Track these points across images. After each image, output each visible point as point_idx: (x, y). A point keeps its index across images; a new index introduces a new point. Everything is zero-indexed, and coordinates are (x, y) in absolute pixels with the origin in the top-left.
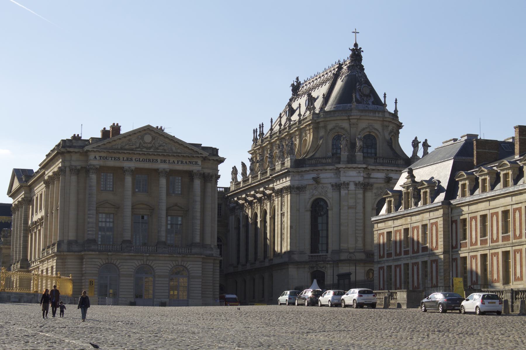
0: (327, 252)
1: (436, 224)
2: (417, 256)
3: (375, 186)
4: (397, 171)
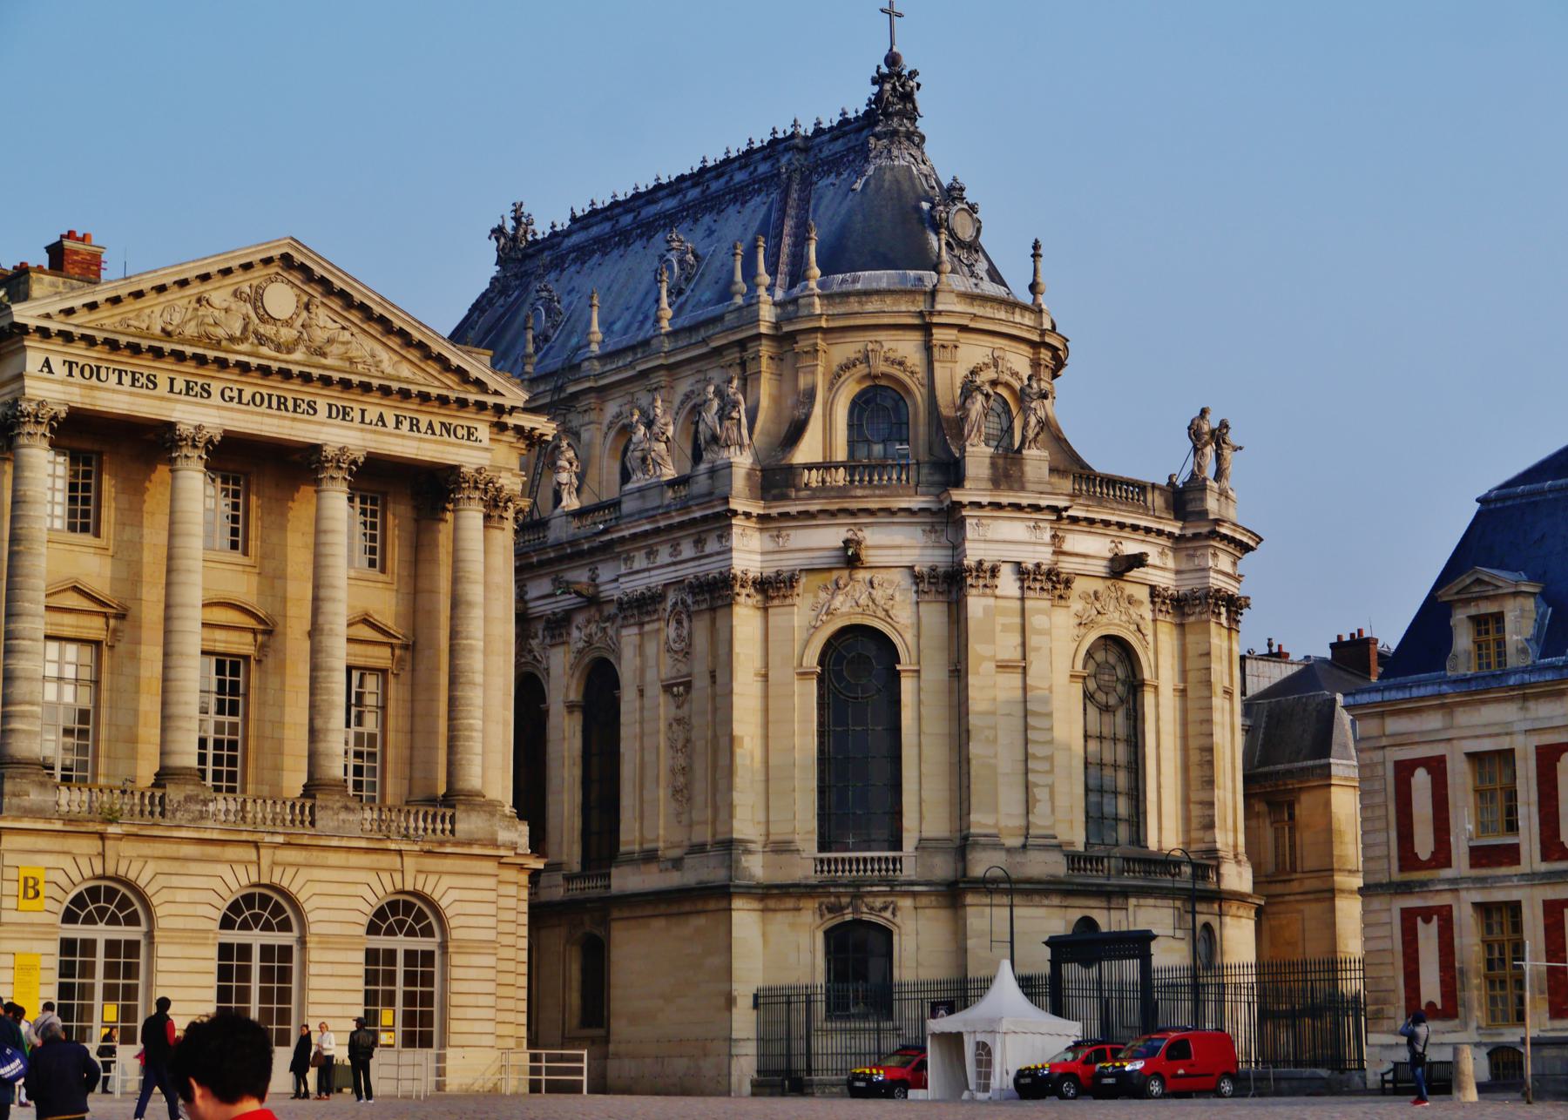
0: (897, 844)
3: (1079, 585)
4: (1148, 530)
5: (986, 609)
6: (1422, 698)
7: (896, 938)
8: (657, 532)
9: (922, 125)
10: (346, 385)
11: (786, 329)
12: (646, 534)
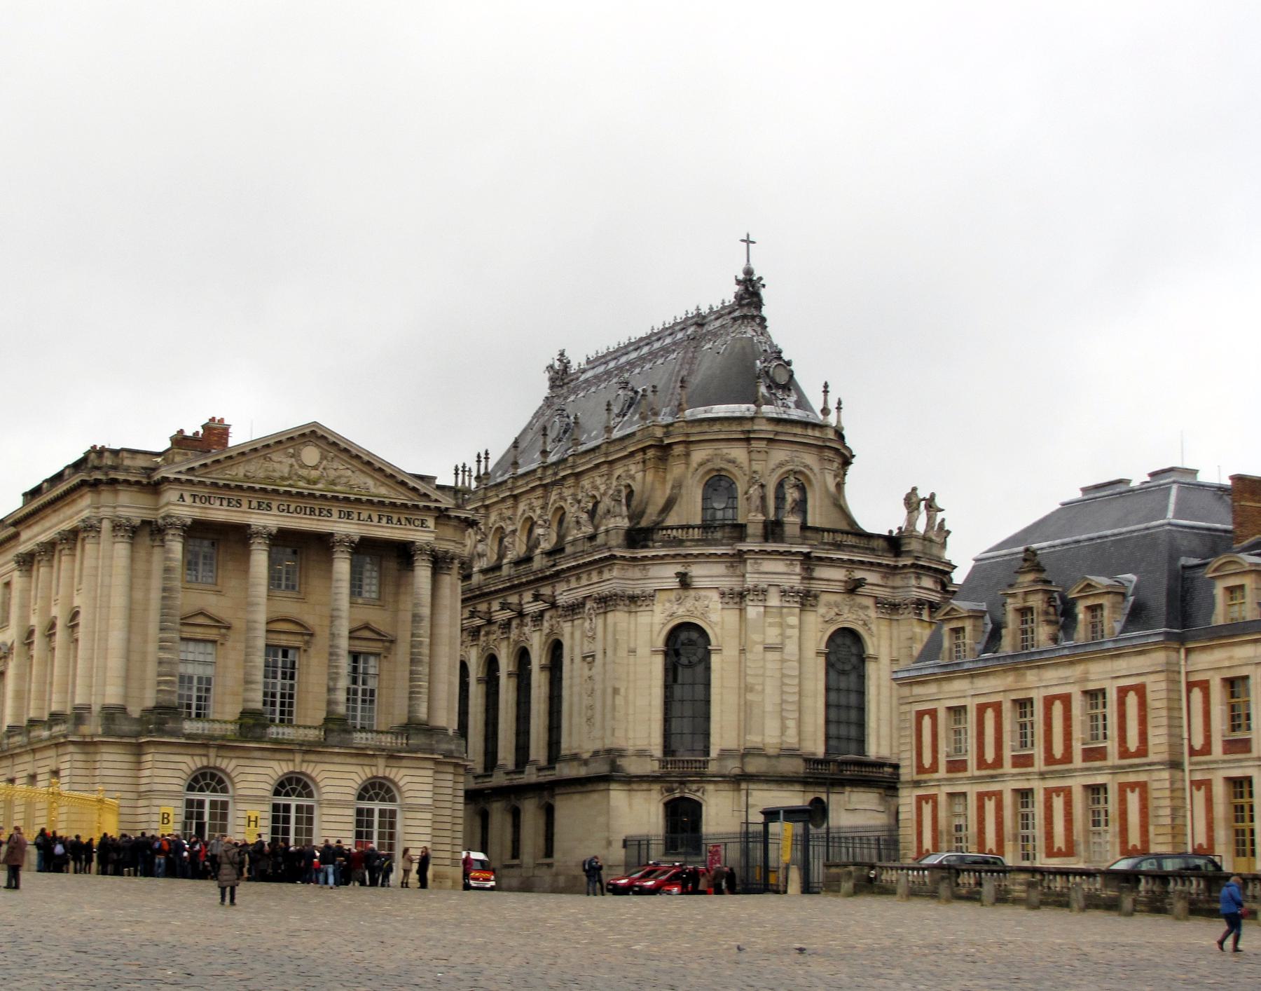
1: (1140, 690)
2: (1068, 771)
3: (825, 598)
4: (871, 564)
5: (758, 614)
6: (926, 675)
7: (704, 808)
8: (579, 566)
9: (765, 311)
10: (347, 500)
12: (574, 568)
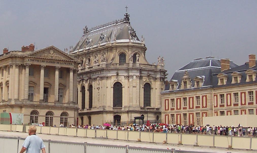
1: (206, 96)
3: (143, 77)
4: (152, 71)
7: (121, 117)
9: (130, 21)
11: (112, 47)
